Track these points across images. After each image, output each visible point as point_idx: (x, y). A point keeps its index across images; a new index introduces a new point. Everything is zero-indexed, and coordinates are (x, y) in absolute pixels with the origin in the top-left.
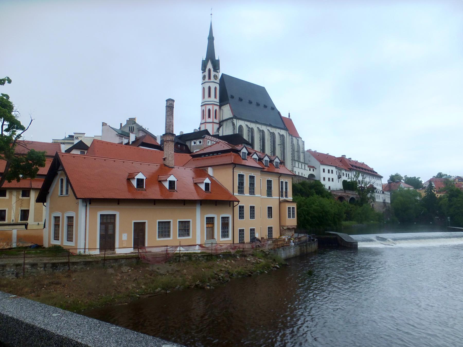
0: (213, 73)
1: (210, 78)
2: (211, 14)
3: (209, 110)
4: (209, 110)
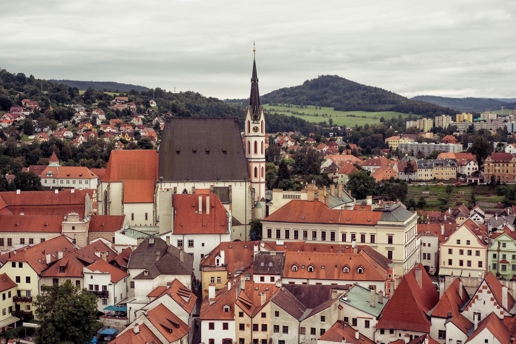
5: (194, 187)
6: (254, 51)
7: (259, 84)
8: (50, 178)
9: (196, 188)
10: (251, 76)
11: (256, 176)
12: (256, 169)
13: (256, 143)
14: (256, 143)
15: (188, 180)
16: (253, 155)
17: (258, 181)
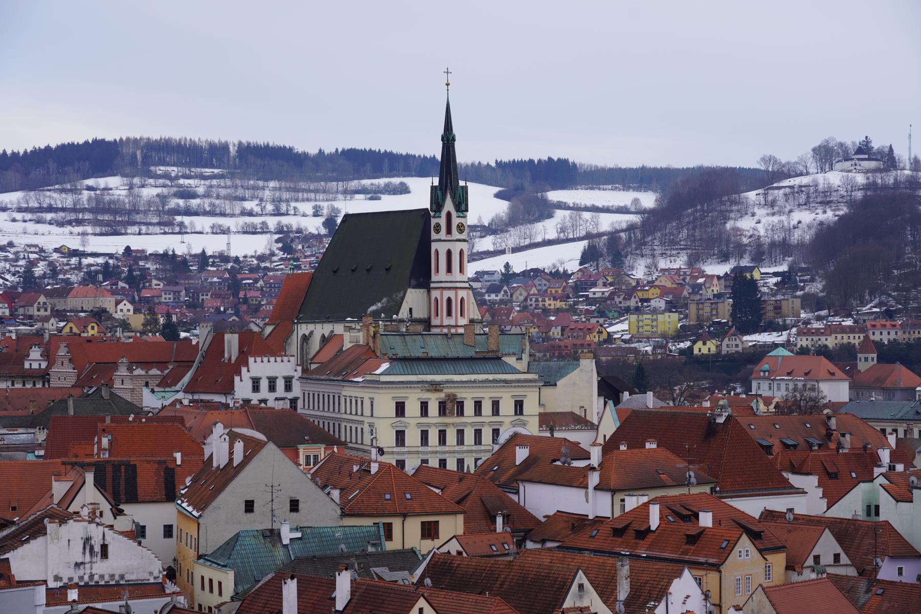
0: (455, 221)
1: (449, 231)
2: (448, 85)
3: (449, 300)
4: (449, 300)
5: (332, 332)
6: (448, 85)
7: (458, 146)
8: (764, 378)
9: (336, 332)
10: (441, 131)
11: (449, 314)
12: (436, 300)
13: (449, 253)
14: (449, 253)
15: (329, 319)
16: (434, 278)
17: (454, 324)
